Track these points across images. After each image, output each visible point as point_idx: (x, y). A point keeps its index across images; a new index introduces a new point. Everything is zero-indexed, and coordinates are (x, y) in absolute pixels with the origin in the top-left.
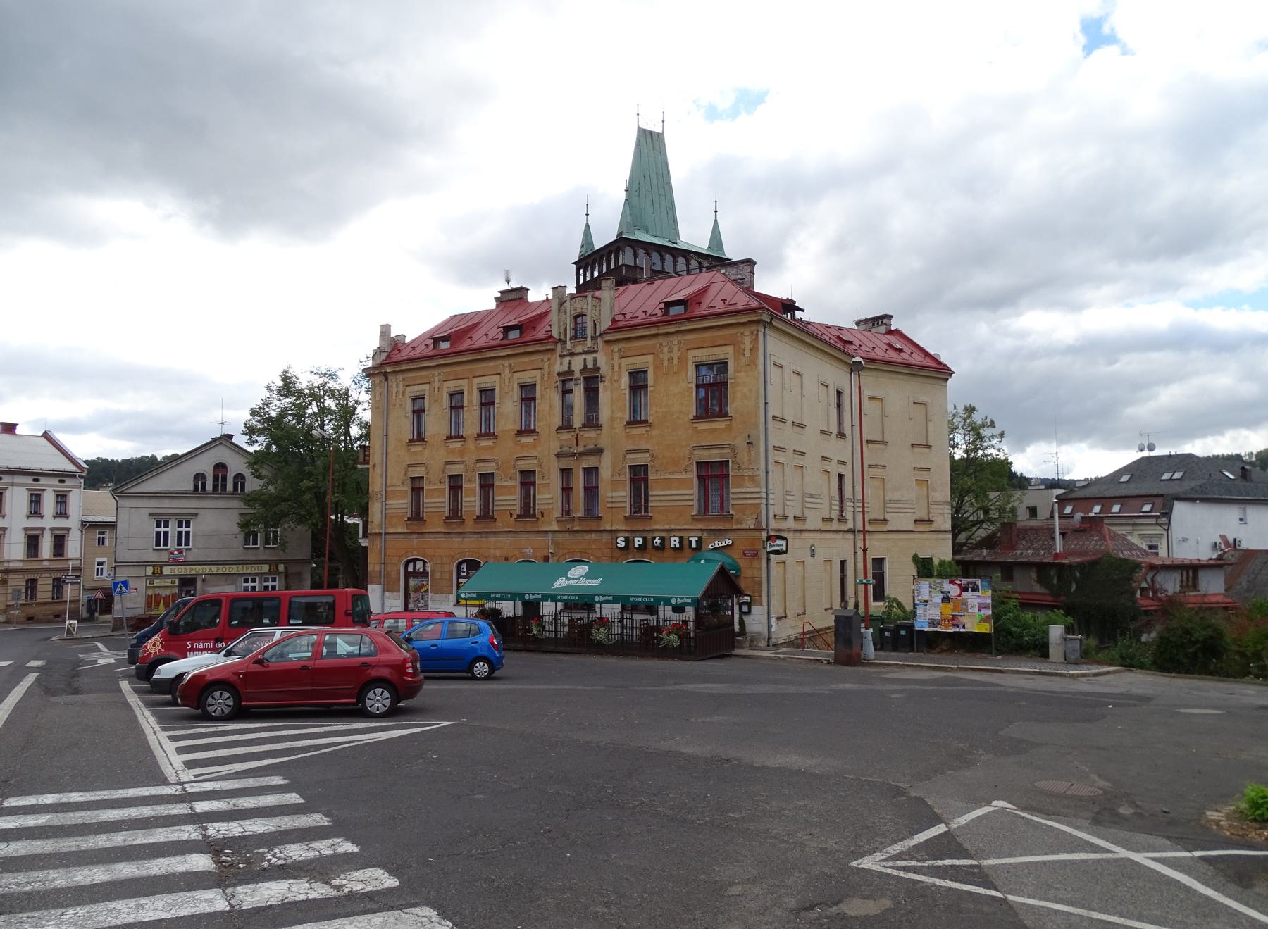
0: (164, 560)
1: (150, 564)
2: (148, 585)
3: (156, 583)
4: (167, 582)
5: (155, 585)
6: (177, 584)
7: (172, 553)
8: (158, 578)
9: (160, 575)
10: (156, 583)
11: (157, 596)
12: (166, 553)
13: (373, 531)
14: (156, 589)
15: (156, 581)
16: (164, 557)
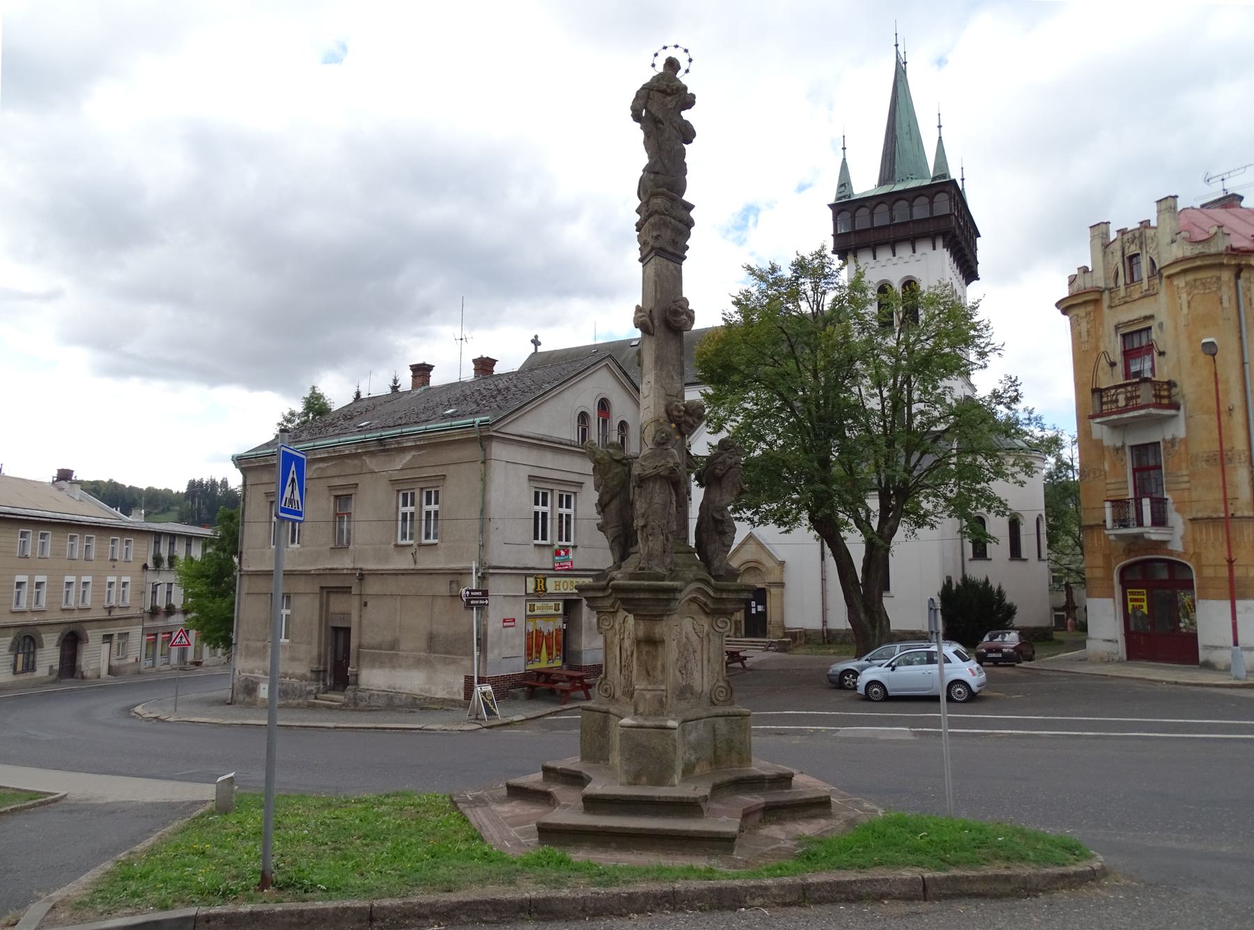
0: (548, 567)
1: (532, 572)
2: (529, 613)
3: (538, 608)
4: (550, 608)
5: (537, 612)
6: (561, 612)
7: (558, 553)
8: (540, 600)
9: (540, 593)
10: (538, 608)
11: (539, 632)
12: (548, 554)
13: (1239, 514)
14: (538, 621)
15: (538, 604)
16: (544, 560)
